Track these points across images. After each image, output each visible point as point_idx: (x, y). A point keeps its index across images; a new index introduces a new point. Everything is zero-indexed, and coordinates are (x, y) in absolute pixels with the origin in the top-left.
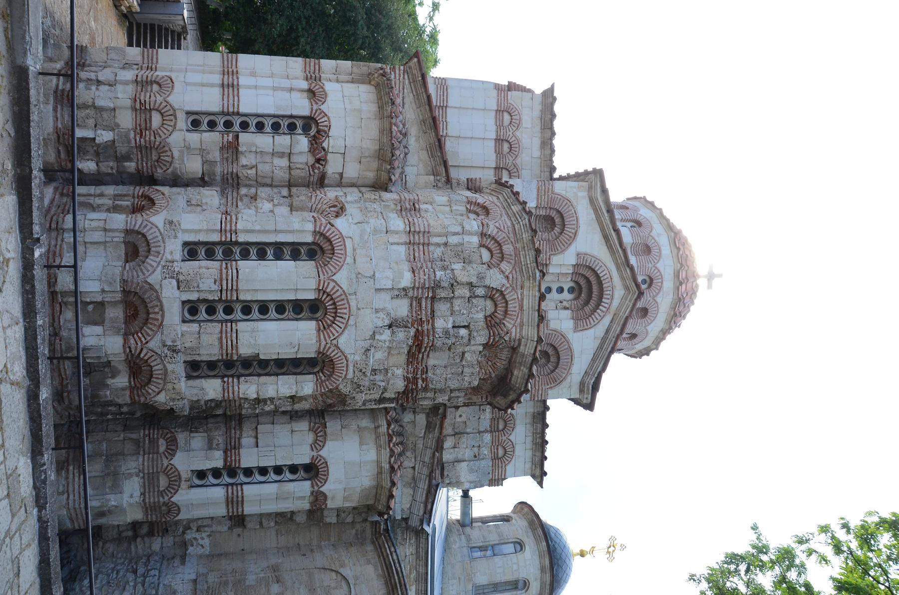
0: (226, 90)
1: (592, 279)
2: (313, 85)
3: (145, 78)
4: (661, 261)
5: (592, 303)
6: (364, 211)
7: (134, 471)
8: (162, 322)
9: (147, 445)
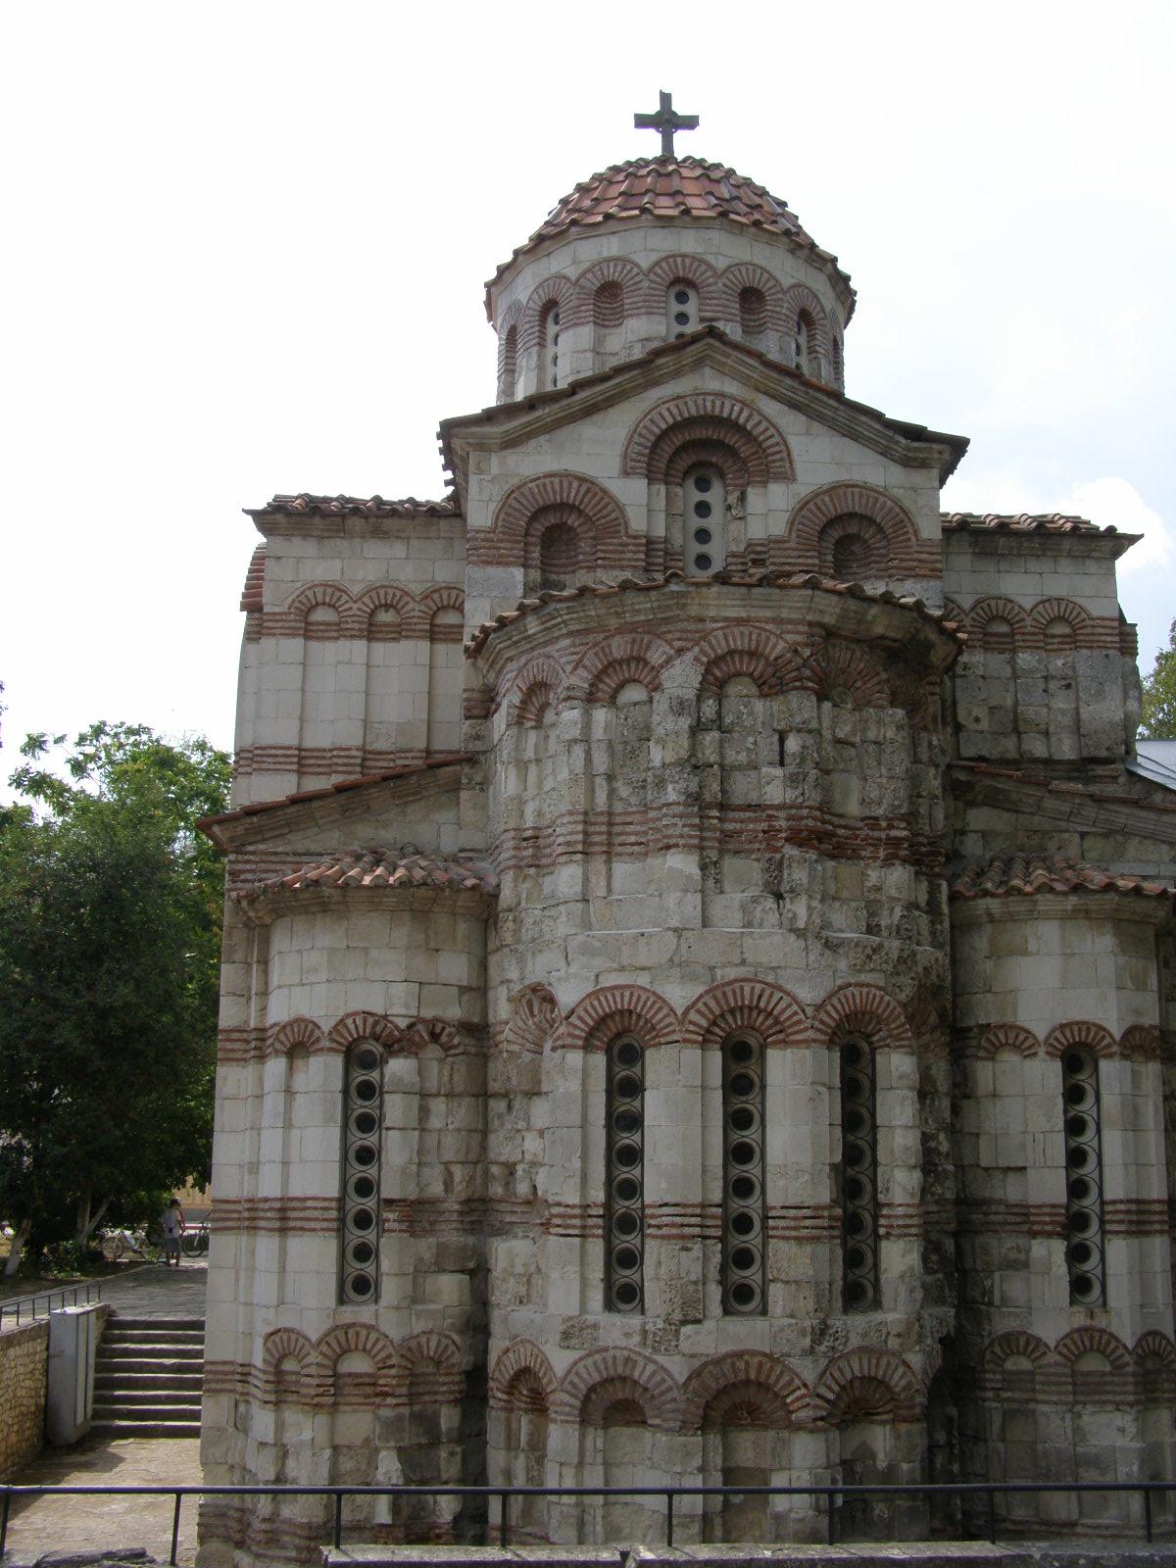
0: (292, 1224)
1: (678, 440)
2: (278, 1046)
3: (269, 1387)
4: (635, 258)
5: (732, 439)
6: (539, 944)
7: (1068, 1423)
8: (765, 1355)
9: (1017, 1395)
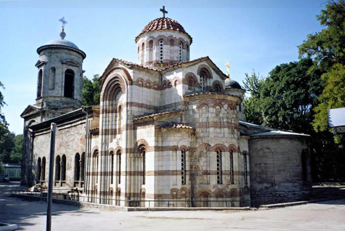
5: (206, 72)
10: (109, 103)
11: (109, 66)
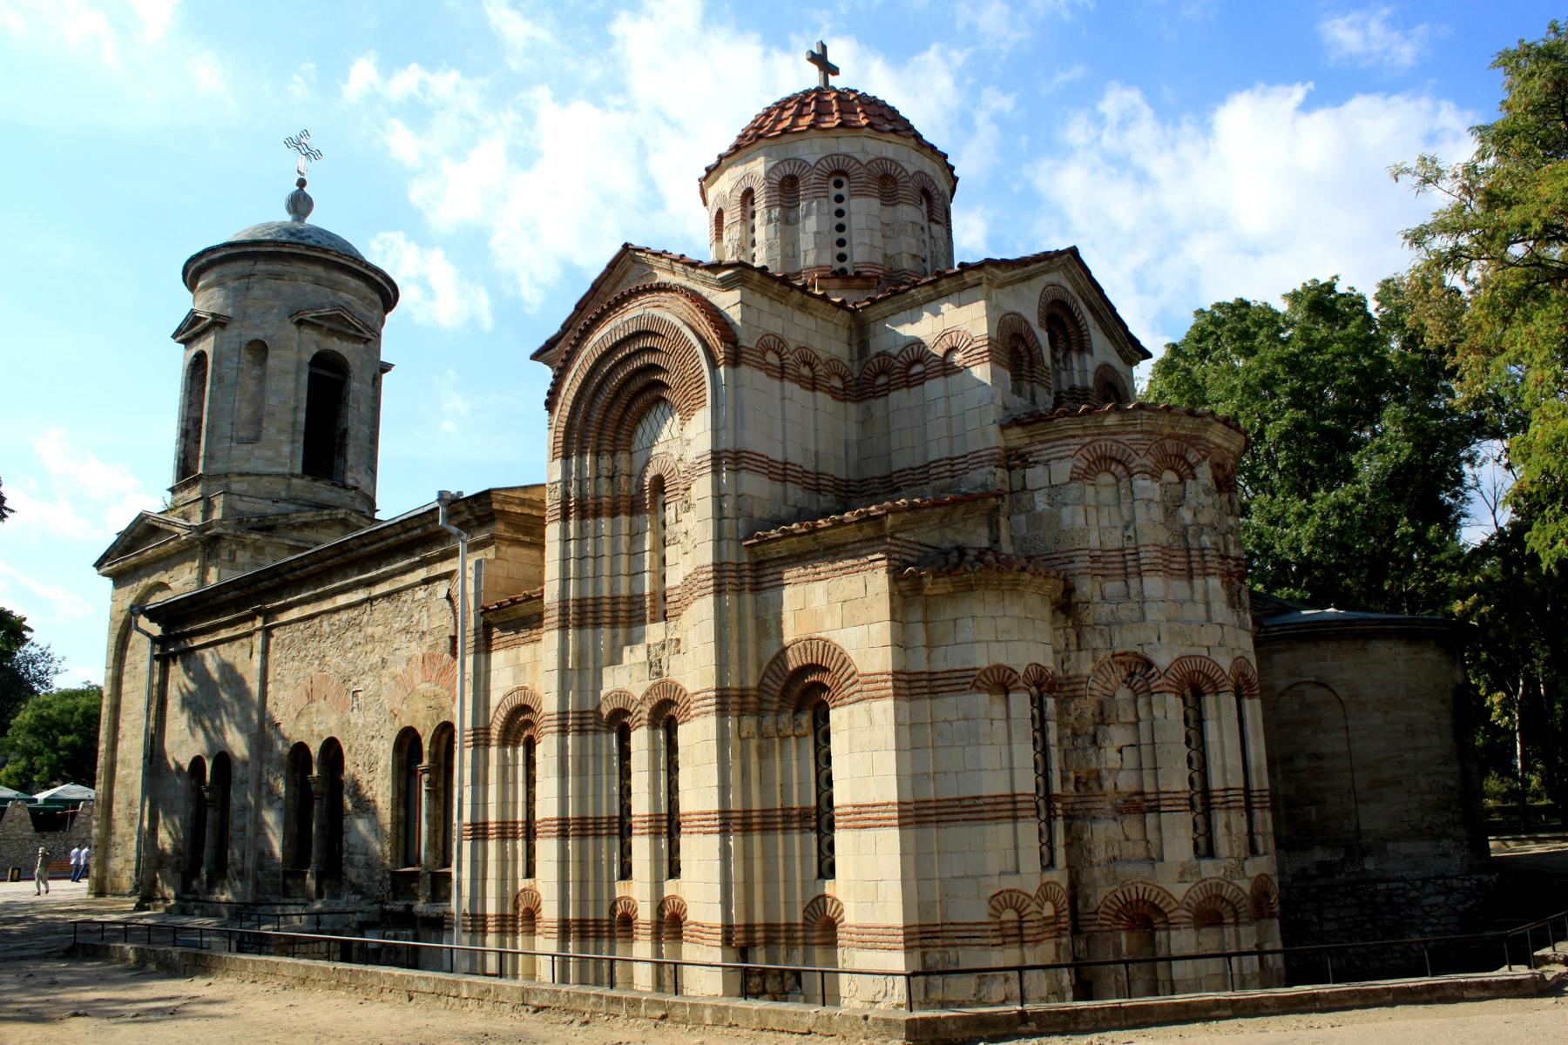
5: (1065, 319)
10: (596, 464)
11: (596, 287)
